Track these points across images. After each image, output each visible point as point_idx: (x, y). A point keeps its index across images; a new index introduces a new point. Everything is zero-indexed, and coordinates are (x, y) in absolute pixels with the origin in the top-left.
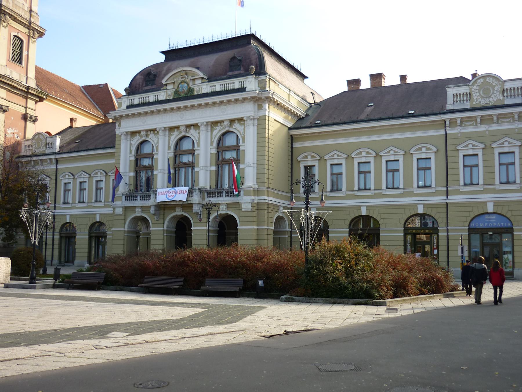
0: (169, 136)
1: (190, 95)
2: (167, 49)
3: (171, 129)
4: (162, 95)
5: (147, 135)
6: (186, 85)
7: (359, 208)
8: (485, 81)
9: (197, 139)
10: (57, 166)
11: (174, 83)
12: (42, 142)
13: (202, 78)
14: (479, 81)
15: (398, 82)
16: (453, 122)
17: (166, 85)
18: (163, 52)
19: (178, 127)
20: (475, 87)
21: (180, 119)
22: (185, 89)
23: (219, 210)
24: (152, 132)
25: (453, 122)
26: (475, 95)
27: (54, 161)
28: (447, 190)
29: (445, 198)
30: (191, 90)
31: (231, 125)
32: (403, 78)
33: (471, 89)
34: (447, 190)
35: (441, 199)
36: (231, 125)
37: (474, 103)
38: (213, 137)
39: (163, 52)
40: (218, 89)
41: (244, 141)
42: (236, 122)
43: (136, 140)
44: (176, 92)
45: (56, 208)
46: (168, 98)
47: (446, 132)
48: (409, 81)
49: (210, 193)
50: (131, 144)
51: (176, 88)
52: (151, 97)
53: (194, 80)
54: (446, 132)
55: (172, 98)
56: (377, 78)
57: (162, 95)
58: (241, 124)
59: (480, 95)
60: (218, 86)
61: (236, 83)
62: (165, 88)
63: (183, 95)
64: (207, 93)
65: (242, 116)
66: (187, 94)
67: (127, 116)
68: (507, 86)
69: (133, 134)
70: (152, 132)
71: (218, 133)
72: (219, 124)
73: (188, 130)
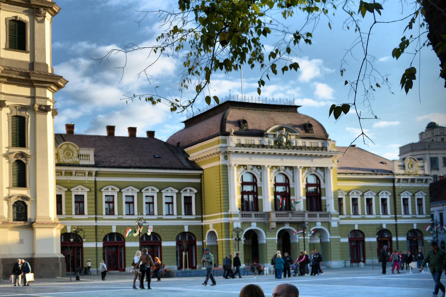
5: (252, 169)
7: (354, 225)
12: (73, 153)
16: (399, 180)
23: (315, 225)
29: (394, 221)
31: (315, 171)
35: (393, 221)
41: (324, 182)
42: (319, 169)
47: (394, 185)
54: (394, 185)
58: (321, 171)
70: (255, 167)
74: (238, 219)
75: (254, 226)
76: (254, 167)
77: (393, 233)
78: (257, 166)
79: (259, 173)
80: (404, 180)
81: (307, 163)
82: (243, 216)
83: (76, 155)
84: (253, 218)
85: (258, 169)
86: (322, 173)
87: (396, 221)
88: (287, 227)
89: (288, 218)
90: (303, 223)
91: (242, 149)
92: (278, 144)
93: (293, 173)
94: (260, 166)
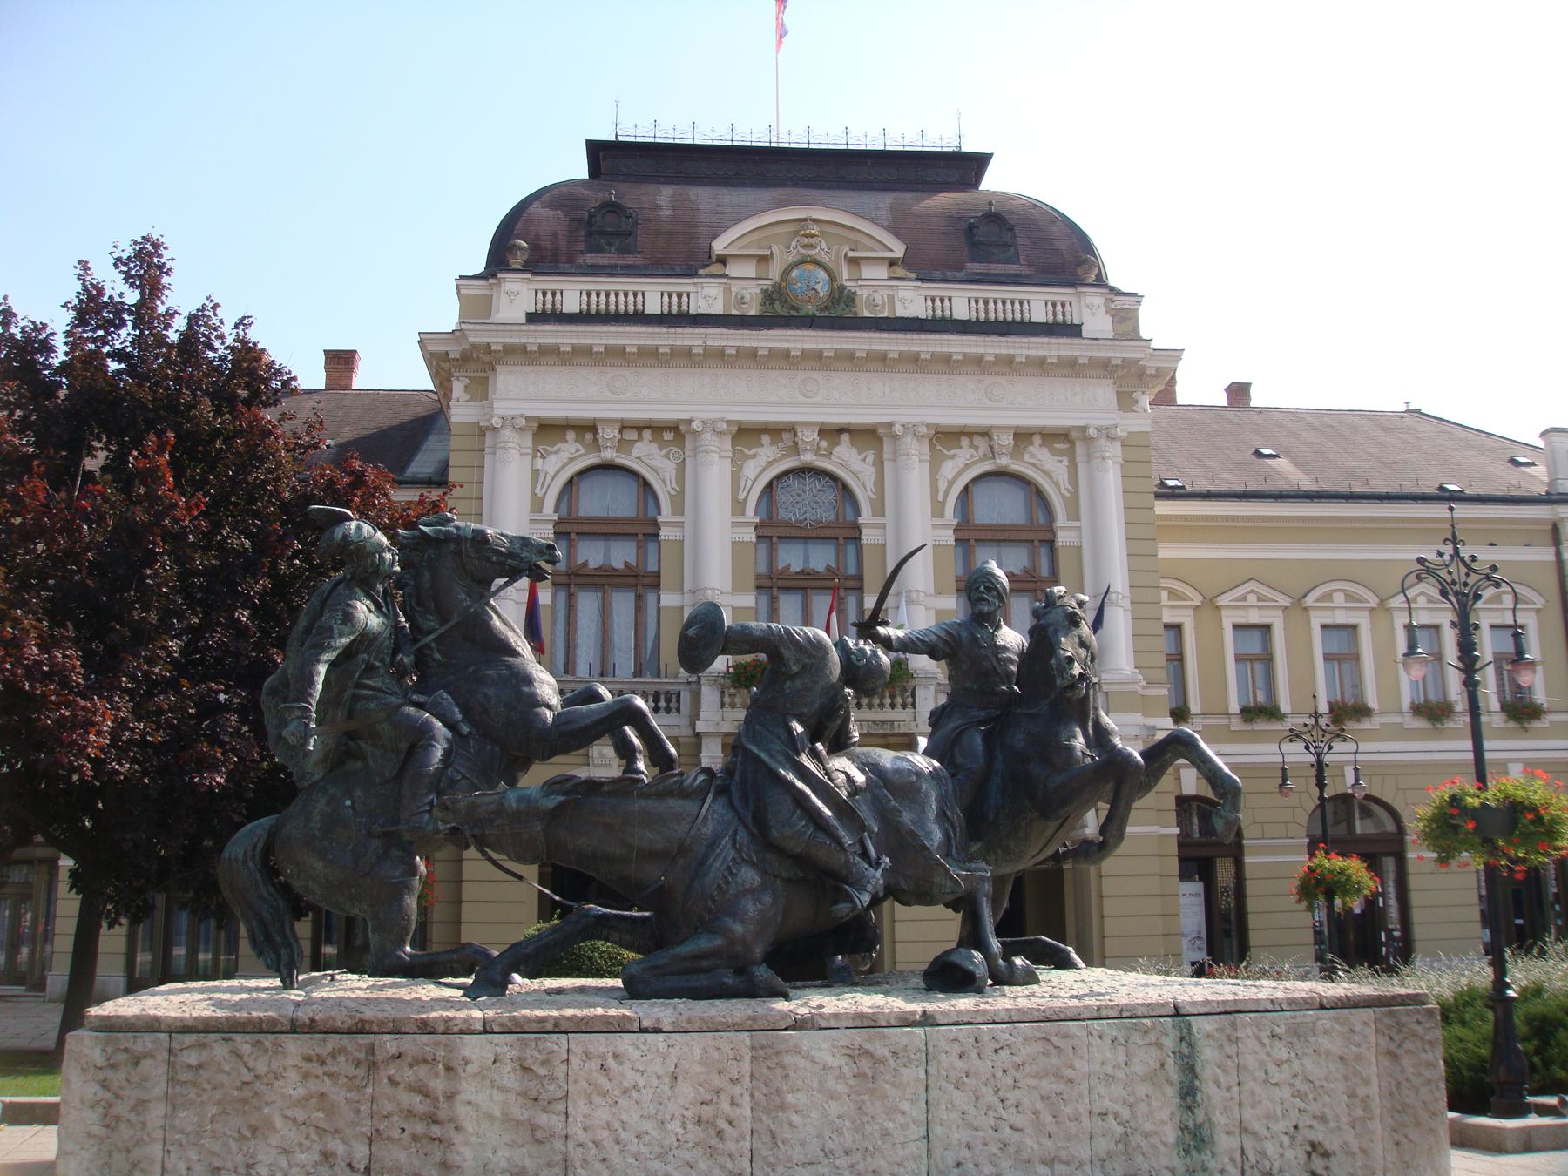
0: (738, 461)
1: (838, 314)
2: (608, 136)
3: (747, 434)
4: (707, 296)
5: (624, 446)
6: (822, 274)
9: (870, 485)
11: (763, 260)
15: (1223, 400)
17: (723, 260)
19: (775, 431)
21: (801, 399)
22: (823, 289)
24: (647, 434)
30: (841, 297)
32: (1239, 392)
36: (1017, 452)
38: (942, 485)
40: (961, 312)
42: (1037, 440)
43: (564, 456)
44: (769, 297)
46: (735, 312)
48: (1257, 399)
50: (536, 472)
51: (776, 278)
52: (654, 295)
53: (854, 262)
55: (753, 313)
57: (707, 296)
58: (1054, 452)
60: (962, 302)
61: (1037, 304)
62: (715, 269)
63: (810, 309)
64: (917, 319)
65: (1081, 423)
66: (826, 308)
67: (550, 354)
69: (548, 430)
70: (647, 434)
72: (965, 441)
73: (824, 444)
76: (640, 438)
78: (657, 429)
81: (961, 402)
85: (663, 445)
92: (779, 312)
93: (879, 464)
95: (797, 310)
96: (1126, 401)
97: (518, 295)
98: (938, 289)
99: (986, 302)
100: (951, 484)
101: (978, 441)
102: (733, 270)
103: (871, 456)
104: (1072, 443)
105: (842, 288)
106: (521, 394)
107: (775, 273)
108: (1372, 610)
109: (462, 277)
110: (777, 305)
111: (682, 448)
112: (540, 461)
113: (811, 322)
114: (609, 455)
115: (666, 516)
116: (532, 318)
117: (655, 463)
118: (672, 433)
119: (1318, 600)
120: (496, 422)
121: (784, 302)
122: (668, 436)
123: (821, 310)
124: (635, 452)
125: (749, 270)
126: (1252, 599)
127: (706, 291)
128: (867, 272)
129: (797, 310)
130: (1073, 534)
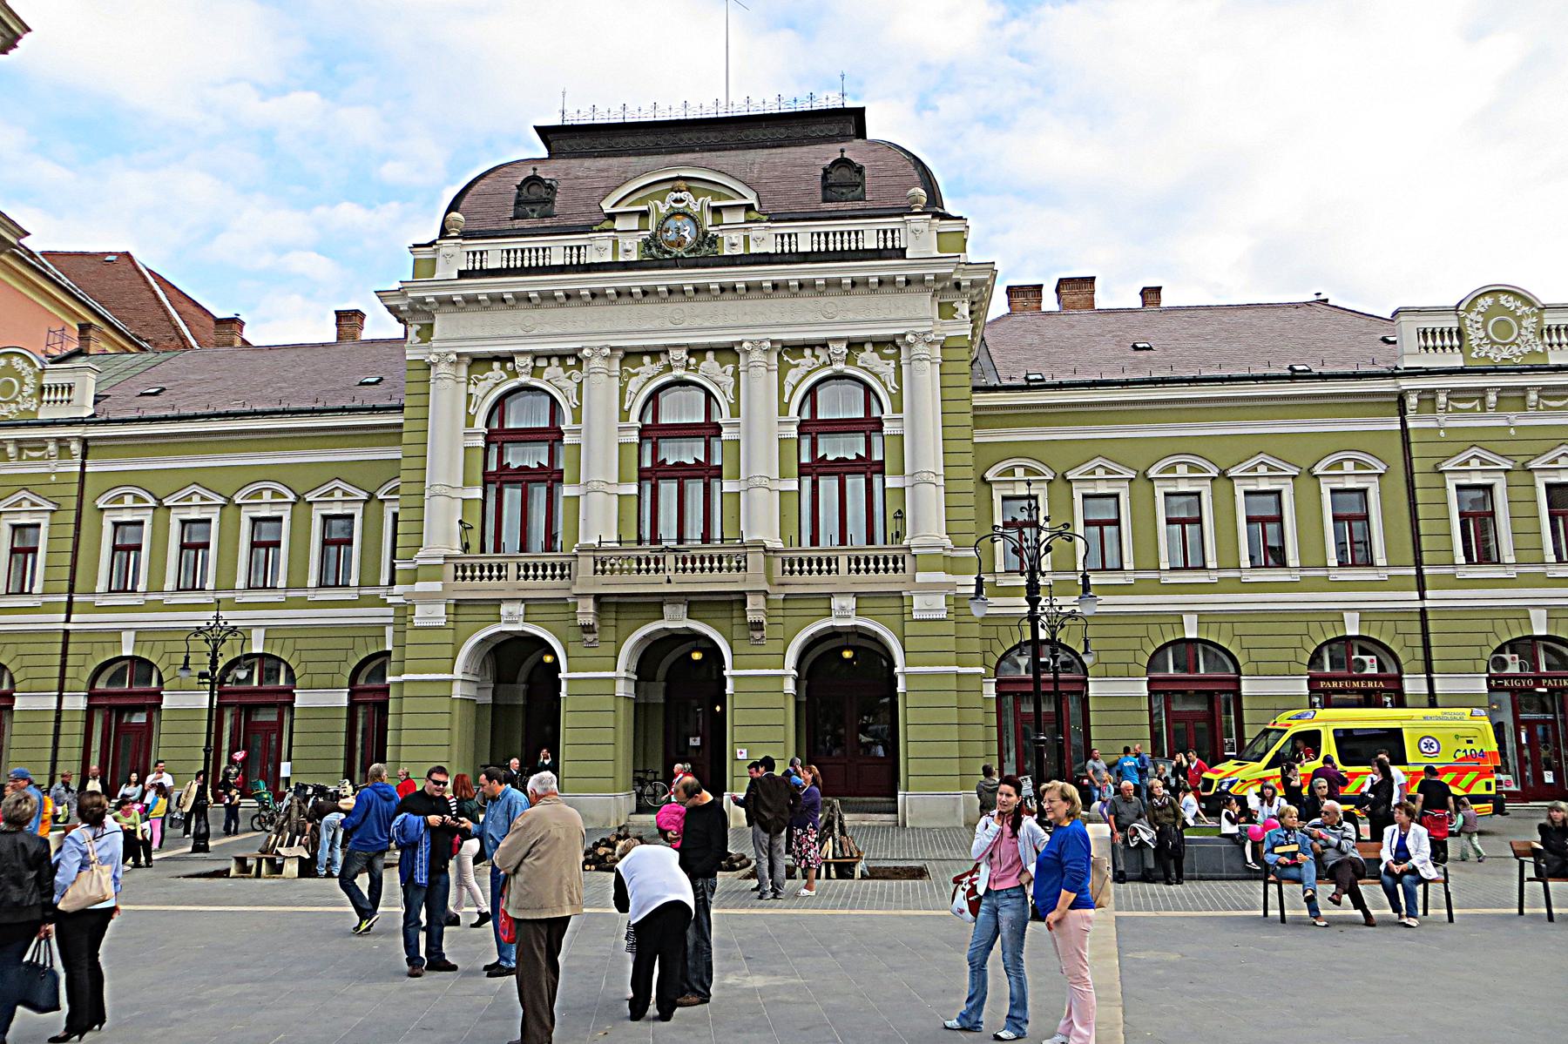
1: (705, 253)
2: (555, 121)
4: (598, 249)
5: (536, 372)
8: (1497, 301)
9: (730, 392)
10: (83, 466)
11: (644, 215)
12: (22, 384)
13: (749, 208)
14: (1481, 301)
16: (1428, 398)
18: (543, 132)
20: (1472, 315)
22: (689, 233)
25: (1428, 398)
26: (1474, 335)
27: (75, 447)
28: (1420, 576)
29: (1416, 595)
32: (1151, 294)
33: (1461, 320)
34: (1420, 576)
37: (1474, 355)
38: (788, 390)
39: (543, 132)
45: (75, 608)
47: (1403, 423)
48: (1167, 300)
49: (792, 565)
53: (717, 211)
54: (1403, 423)
56: (1077, 288)
57: (598, 249)
58: (883, 357)
59: (1487, 335)
66: (693, 250)
68: (1550, 320)
69: (479, 362)
70: (555, 361)
71: (804, 378)
72: (807, 352)
73: (693, 361)
74: (437, 586)
75: (513, 620)
77: (1410, 656)
79: (571, 386)
80: (1453, 394)
82: (463, 571)
83: (28, 390)
84: (512, 583)
86: (888, 369)
87: (1422, 598)
88: (676, 620)
89: (662, 577)
90: (738, 600)
91: (482, 288)
92: (656, 256)
94: (574, 354)
95: (670, 253)
96: (947, 311)
97: (456, 257)
98: (786, 228)
99: (827, 235)
100: (795, 388)
101: (818, 351)
102: (619, 224)
103: (730, 368)
104: (899, 348)
105: (705, 234)
106: (457, 334)
107: (652, 224)
108: (1214, 478)
109: (416, 246)
110: (654, 250)
111: (580, 370)
112: (472, 387)
113: (678, 262)
114: (524, 379)
115: (567, 424)
116: (462, 274)
117: (559, 384)
118: (571, 359)
119: (1163, 471)
120: (433, 358)
121: (659, 247)
122: (571, 362)
123: (689, 252)
124: (545, 376)
125: (634, 223)
126: (1262, 470)
127: (598, 243)
128: (727, 217)
129: (670, 253)
130: (898, 424)
